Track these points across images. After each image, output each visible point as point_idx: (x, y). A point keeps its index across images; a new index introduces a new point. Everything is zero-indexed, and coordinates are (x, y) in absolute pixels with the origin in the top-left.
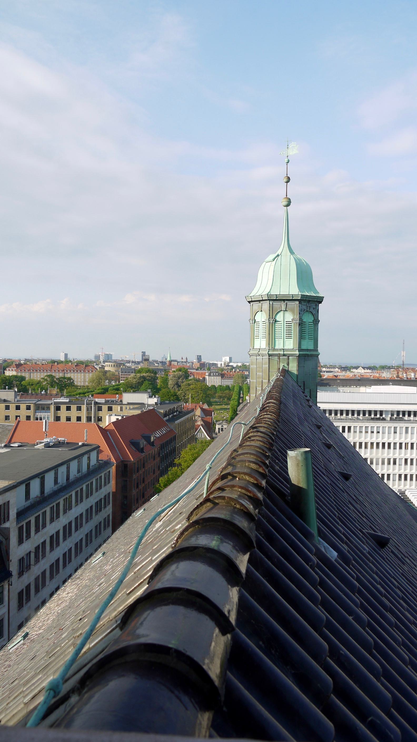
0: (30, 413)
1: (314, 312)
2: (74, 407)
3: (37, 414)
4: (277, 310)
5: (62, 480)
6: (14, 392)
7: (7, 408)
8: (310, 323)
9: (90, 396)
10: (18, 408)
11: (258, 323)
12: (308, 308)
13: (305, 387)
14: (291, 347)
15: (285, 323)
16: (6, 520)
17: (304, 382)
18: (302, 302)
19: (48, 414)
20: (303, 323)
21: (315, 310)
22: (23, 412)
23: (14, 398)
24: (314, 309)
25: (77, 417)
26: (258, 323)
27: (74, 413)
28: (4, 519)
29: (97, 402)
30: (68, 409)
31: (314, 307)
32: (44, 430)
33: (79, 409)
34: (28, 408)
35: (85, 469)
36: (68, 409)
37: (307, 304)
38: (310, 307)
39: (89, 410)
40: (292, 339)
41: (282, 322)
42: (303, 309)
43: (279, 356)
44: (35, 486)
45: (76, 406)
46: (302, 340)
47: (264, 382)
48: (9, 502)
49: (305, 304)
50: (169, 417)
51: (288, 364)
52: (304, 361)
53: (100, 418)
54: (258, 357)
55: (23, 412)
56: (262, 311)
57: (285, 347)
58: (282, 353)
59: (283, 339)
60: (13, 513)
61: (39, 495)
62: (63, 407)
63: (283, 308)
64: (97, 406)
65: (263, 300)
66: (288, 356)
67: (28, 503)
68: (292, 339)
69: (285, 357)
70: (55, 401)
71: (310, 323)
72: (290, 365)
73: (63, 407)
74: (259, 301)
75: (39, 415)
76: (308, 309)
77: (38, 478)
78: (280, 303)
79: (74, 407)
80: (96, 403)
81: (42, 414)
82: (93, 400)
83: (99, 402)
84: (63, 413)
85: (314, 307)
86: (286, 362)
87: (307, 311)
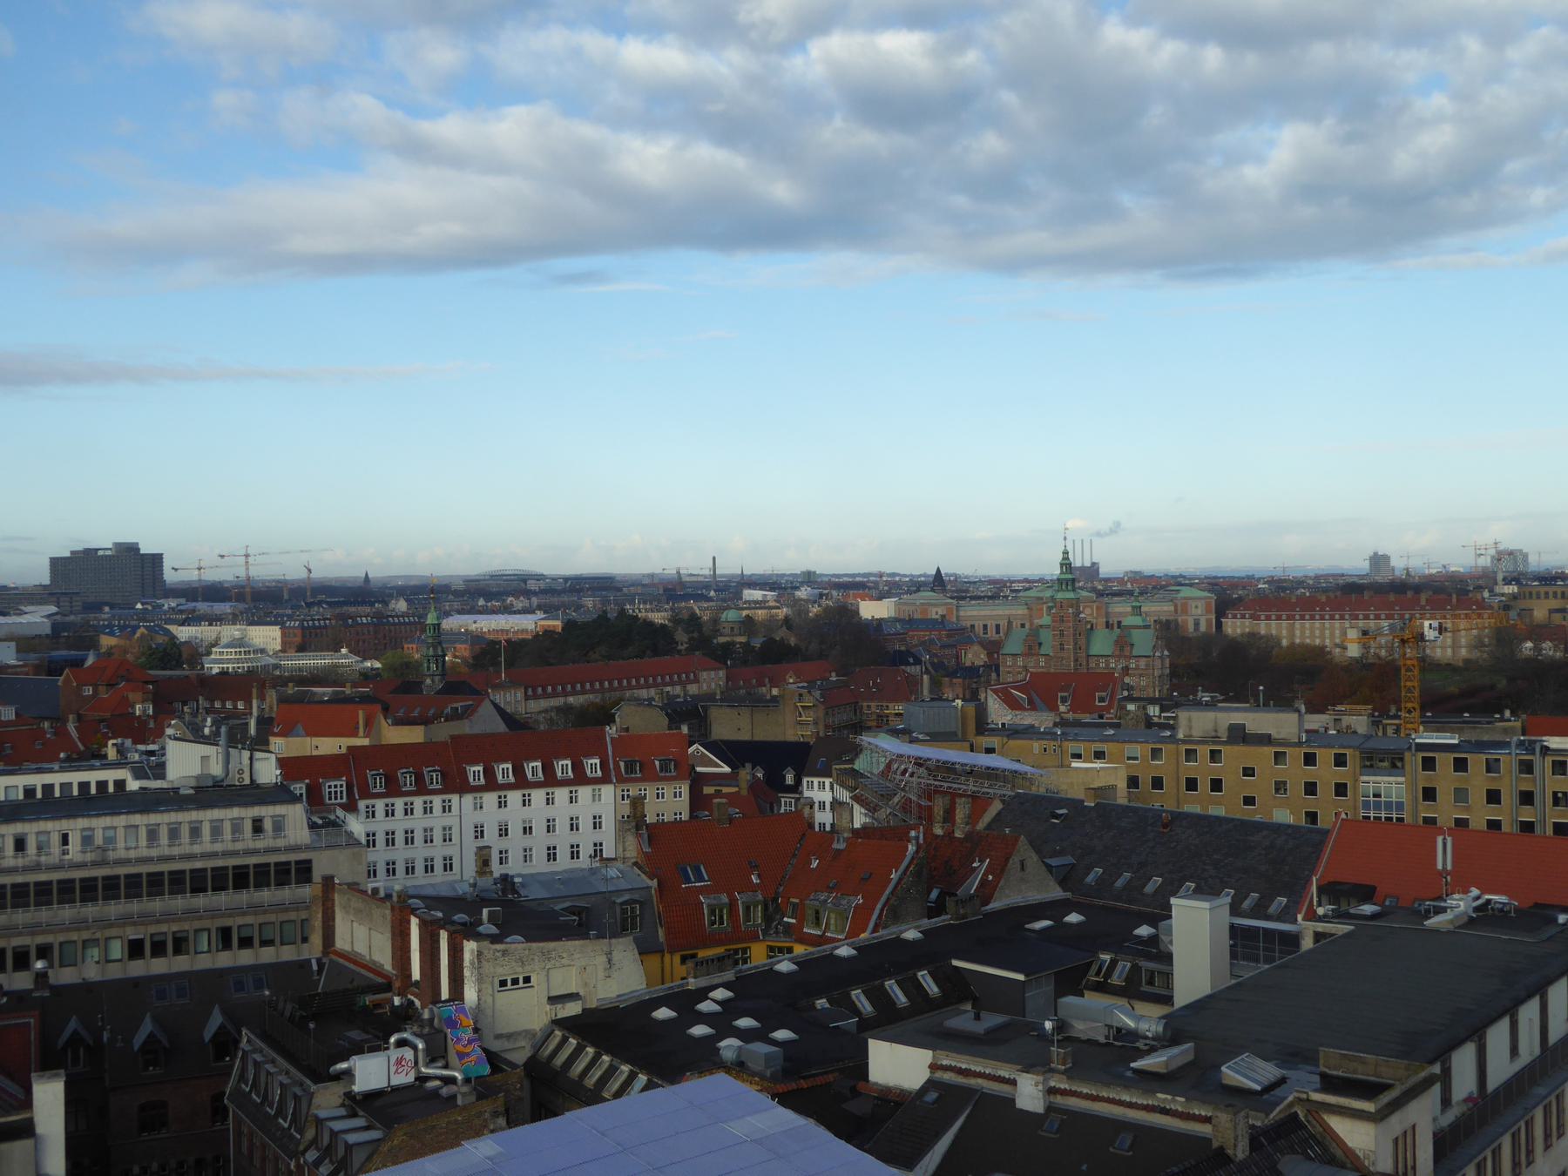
2: (1477, 761)
7: (1279, 757)
9: (1507, 713)
10: (1310, 759)
23: (1296, 730)
25: (1489, 791)
29: (1547, 748)
30: (1461, 765)
32: (1440, 867)
34: (1340, 761)
36: (1461, 765)
39: (1527, 767)
48: (1414, 1126)
62: (1445, 761)
64: (1549, 760)
70: (1417, 741)
73: (1445, 761)
81: (1379, 778)
82: (1535, 742)
84: (1445, 777)
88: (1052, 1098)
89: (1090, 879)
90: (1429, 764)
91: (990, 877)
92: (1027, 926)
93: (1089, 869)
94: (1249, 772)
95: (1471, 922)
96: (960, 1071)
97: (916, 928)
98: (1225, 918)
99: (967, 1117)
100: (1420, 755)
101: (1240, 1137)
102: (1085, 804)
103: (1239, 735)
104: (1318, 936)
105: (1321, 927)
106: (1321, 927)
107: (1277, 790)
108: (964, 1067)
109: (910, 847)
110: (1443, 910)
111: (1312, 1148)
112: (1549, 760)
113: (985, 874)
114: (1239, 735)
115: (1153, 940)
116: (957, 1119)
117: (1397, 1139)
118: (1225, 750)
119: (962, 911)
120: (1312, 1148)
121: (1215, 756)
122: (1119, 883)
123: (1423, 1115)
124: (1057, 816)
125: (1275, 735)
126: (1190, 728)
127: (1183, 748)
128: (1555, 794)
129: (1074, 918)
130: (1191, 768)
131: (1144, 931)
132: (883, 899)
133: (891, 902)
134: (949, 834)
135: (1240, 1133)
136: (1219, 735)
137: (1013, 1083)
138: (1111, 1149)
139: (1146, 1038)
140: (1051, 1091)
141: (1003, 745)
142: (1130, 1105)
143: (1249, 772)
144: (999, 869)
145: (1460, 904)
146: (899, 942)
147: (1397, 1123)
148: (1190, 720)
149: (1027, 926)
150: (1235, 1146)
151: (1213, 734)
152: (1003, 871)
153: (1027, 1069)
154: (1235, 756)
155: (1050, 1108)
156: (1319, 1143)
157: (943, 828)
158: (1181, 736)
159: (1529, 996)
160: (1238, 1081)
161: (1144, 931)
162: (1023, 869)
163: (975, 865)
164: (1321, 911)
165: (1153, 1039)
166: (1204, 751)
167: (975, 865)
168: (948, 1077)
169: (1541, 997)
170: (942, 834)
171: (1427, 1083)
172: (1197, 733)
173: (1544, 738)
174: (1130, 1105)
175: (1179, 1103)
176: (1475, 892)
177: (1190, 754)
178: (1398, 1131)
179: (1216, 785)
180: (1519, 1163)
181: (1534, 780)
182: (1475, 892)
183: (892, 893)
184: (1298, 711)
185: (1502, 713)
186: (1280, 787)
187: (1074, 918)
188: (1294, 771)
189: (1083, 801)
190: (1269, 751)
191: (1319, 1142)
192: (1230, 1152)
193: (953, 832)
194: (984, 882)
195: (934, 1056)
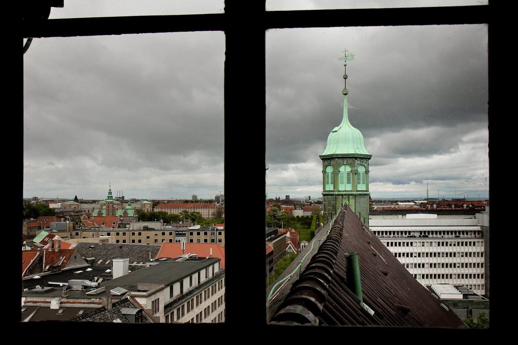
0: (171, 237)
1: (366, 165)
2: (202, 233)
3: (177, 238)
4: (341, 164)
5: (195, 283)
6: (161, 223)
8: (363, 173)
9: (213, 225)
10: (163, 234)
11: (328, 173)
12: (362, 162)
13: (361, 216)
14: (350, 189)
15: (346, 173)
16: (157, 311)
17: (360, 212)
18: (357, 159)
19: (185, 238)
20: (358, 173)
21: (366, 164)
22: (167, 237)
23: (161, 227)
24: (365, 163)
26: (328, 173)
27: (202, 237)
28: (156, 310)
29: (218, 229)
30: (199, 234)
31: (366, 162)
32: (182, 249)
33: (206, 234)
34: (171, 234)
35: (210, 275)
36: (199, 234)
37: (361, 161)
38: (363, 162)
40: (351, 184)
41: (344, 173)
42: (358, 164)
43: (342, 195)
44: (177, 287)
45: (204, 232)
46: (358, 184)
47: (333, 213)
48: (158, 299)
49: (360, 160)
50: (268, 238)
51: (349, 201)
52: (360, 199)
53: (220, 240)
54: (328, 197)
55: (167, 237)
56: (330, 165)
57: (346, 189)
58: (344, 193)
59: (344, 184)
60: (162, 307)
61: (180, 294)
62: (195, 233)
63: (345, 163)
65: (331, 158)
66: (349, 195)
67: (172, 300)
68: (351, 184)
69: (346, 196)
71: (363, 173)
72: (351, 201)
73: (195, 233)
74: (329, 159)
75: (178, 238)
76: (362, 163)
77: (179, 282)
78: (342, 160)
79: (202, 233)
80: (217, 230)
81: (180, 238)
83: (219, 229)
84: (195, 237)
85: (366, 162)
86: (347, 200)
87: (361, 165)
88: (62, 305)
89: (99, 262)
90: (191, 234)
91: (65, 261)
92: (74, 273)
93: (99, 260)
94: (148, 237)
95: (187, 260)
96: (34, 302)
97: (38, 275)
98: (127, 264)
99: (34, 314)
100: (189, 232)
101: (109, 304)
102: (99, 244)
103: (146, 229)
104: (150, 265)
105: (151, 264)
106: (151, 264)
107: (155, 242)
108: (35, 300)
109: (38, 253)
110: (181, 257)
111: (130, 305)
112: (218, 232)
113: (63, 260)
114: (146, 229)
115: (110, 272)
116: (31, 314)
117: (153, 302)
118: (142, 232)
119: (55, 270)
120: (130, 305)
121: (140, 234)
122: (107, 263)
123: (164, 297)
124: (91, 248)
125: (155, 228)
126: (133, 227)
127: (131, 232)
128: (219, 239)
129: (89, 269)
130: (133, 238)
131: (108, 271)
132: (27, 267)
133: (30, 268)
134: (54, 251)
135: (109, 302)
136: (141, 229)
137: (50, 302)
138: (77, 315)
139: (93, 287)
140: (61, 303)
141: (81, 233)
142: (84, 303)
143: (148, 237)
144: (68, 259)
145: (187, 256)
146: (33, 280)
147: (153, 298)
148: (133, 225)
149: (74, 273)
150: (108, 306)
151: (140, 229)
152: (69, 259)
153: (54, 297)
154: (145, 234)
155: (61, 308)
156: (133, 304)
157: (52, 249)
158: (131, 229)
159: (195, 272)
160: (115, 293)
161: (108, 271)
162: (75, 258)
163: (61, 258)
164: (151, 260)
165: (95, 287)
166: (137, 233)
167: (61, 258)
168: (29, 304)
169: (198, 273)
170: (51, 251)
171: (162, 289)
172: (135, 228)
173: (217, 227)
174: (84, 303)
175: (97, 300)
176: (190, 254)
177: (133, 234)
178: (154, 300)
179: (140, 241)
180: (189, 309)
181: (215, 237)
182: (190, 254)
183: (31, 265)
184: (161, 222)
185: (212, 225)
186: (156, 241)
187: (89, 269)
188: (160, 237)
189: (99, 243)
190: (153, 233)
191: (133, 304)
192: (106, 308)
193: (55, 250)
194: (62, 263)
195: (25, 300)
